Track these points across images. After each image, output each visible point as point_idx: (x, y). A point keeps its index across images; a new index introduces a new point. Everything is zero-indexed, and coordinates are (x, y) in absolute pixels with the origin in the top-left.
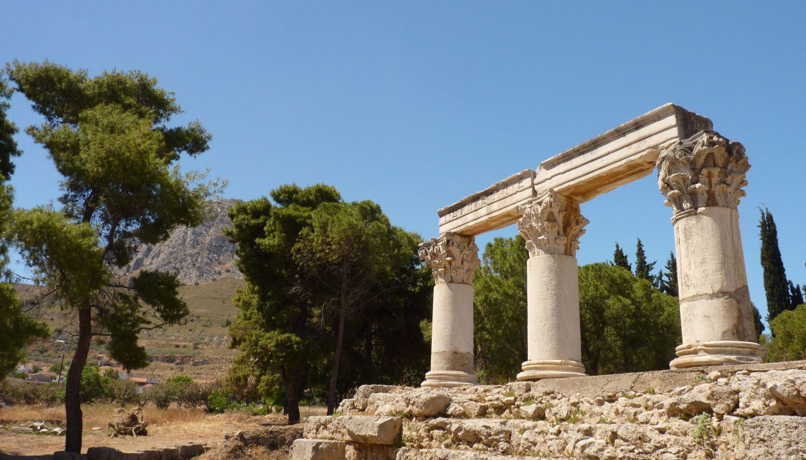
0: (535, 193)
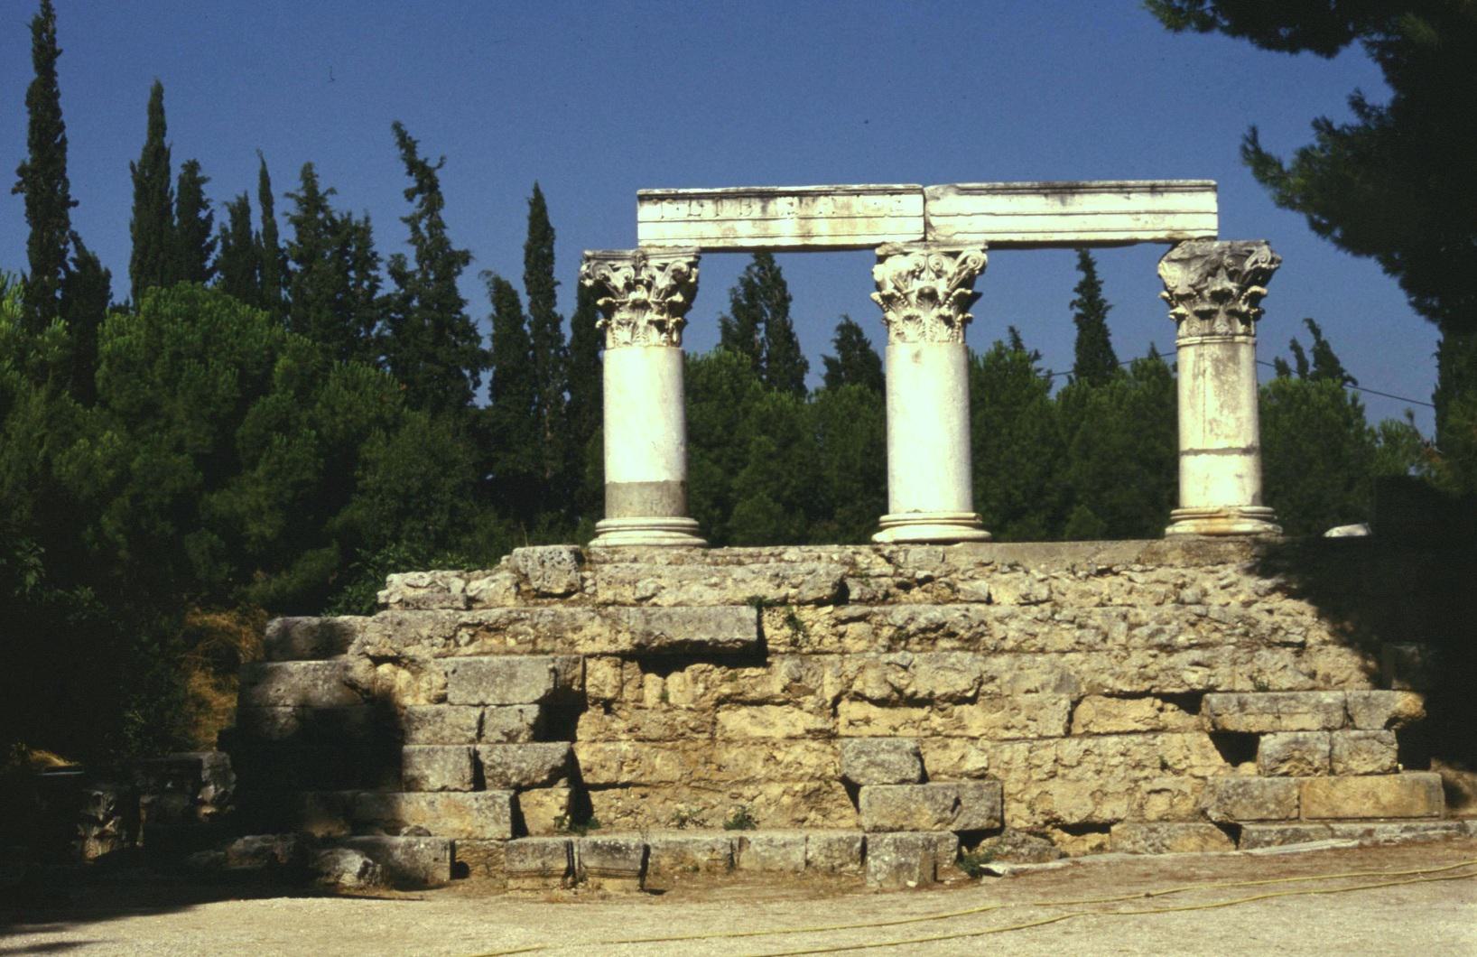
0: (927, 225)
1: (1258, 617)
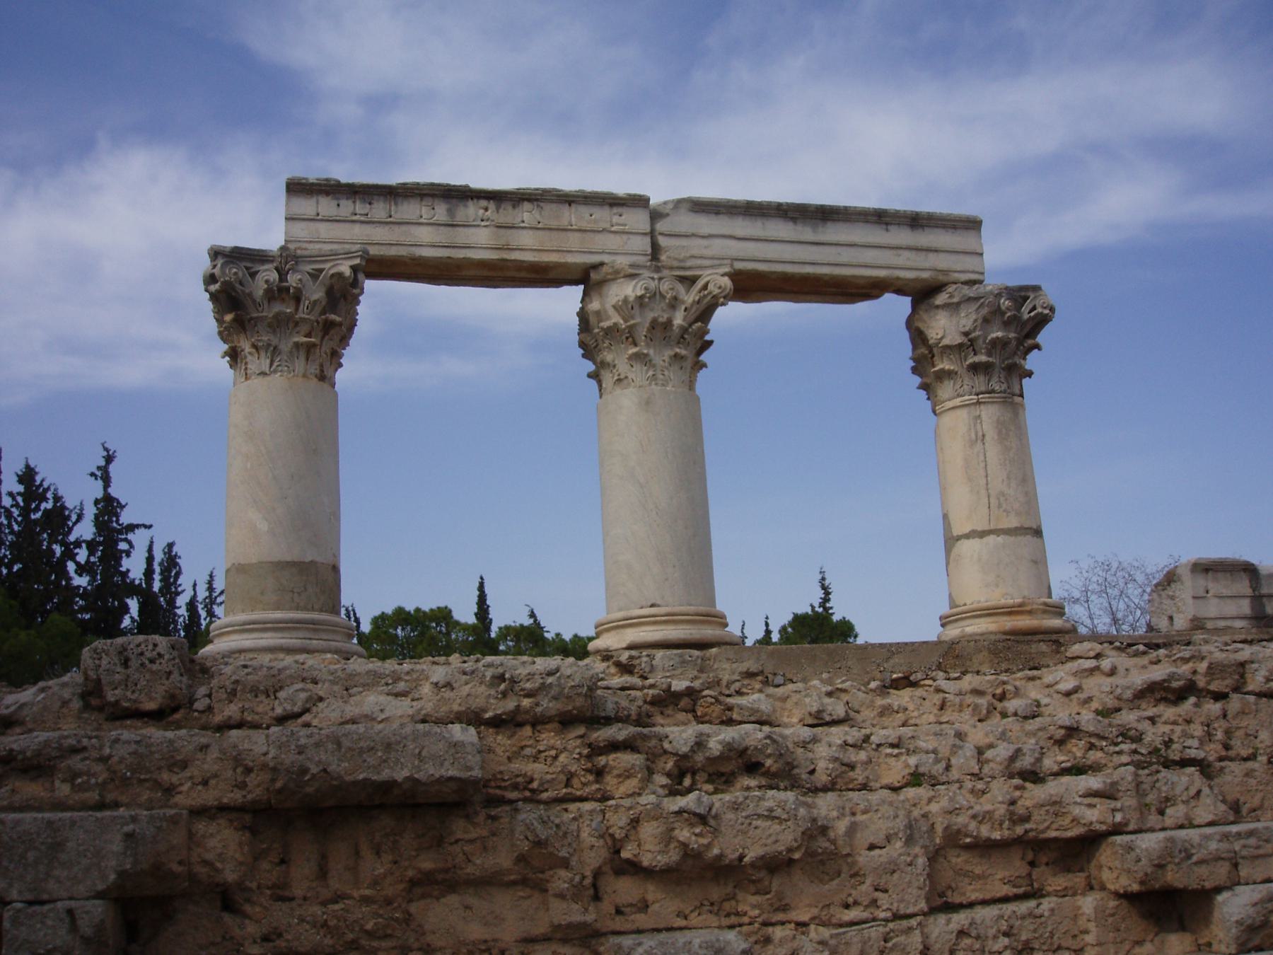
0: (656, 249)
1: (1140, 727)
